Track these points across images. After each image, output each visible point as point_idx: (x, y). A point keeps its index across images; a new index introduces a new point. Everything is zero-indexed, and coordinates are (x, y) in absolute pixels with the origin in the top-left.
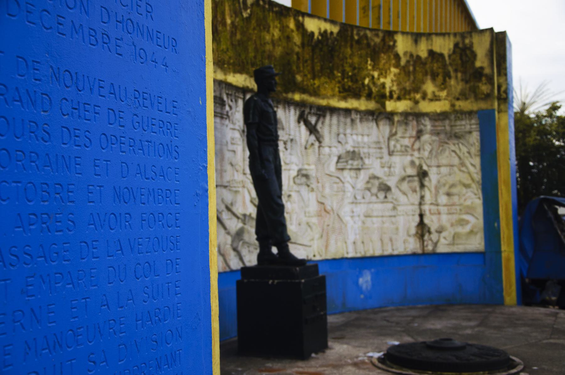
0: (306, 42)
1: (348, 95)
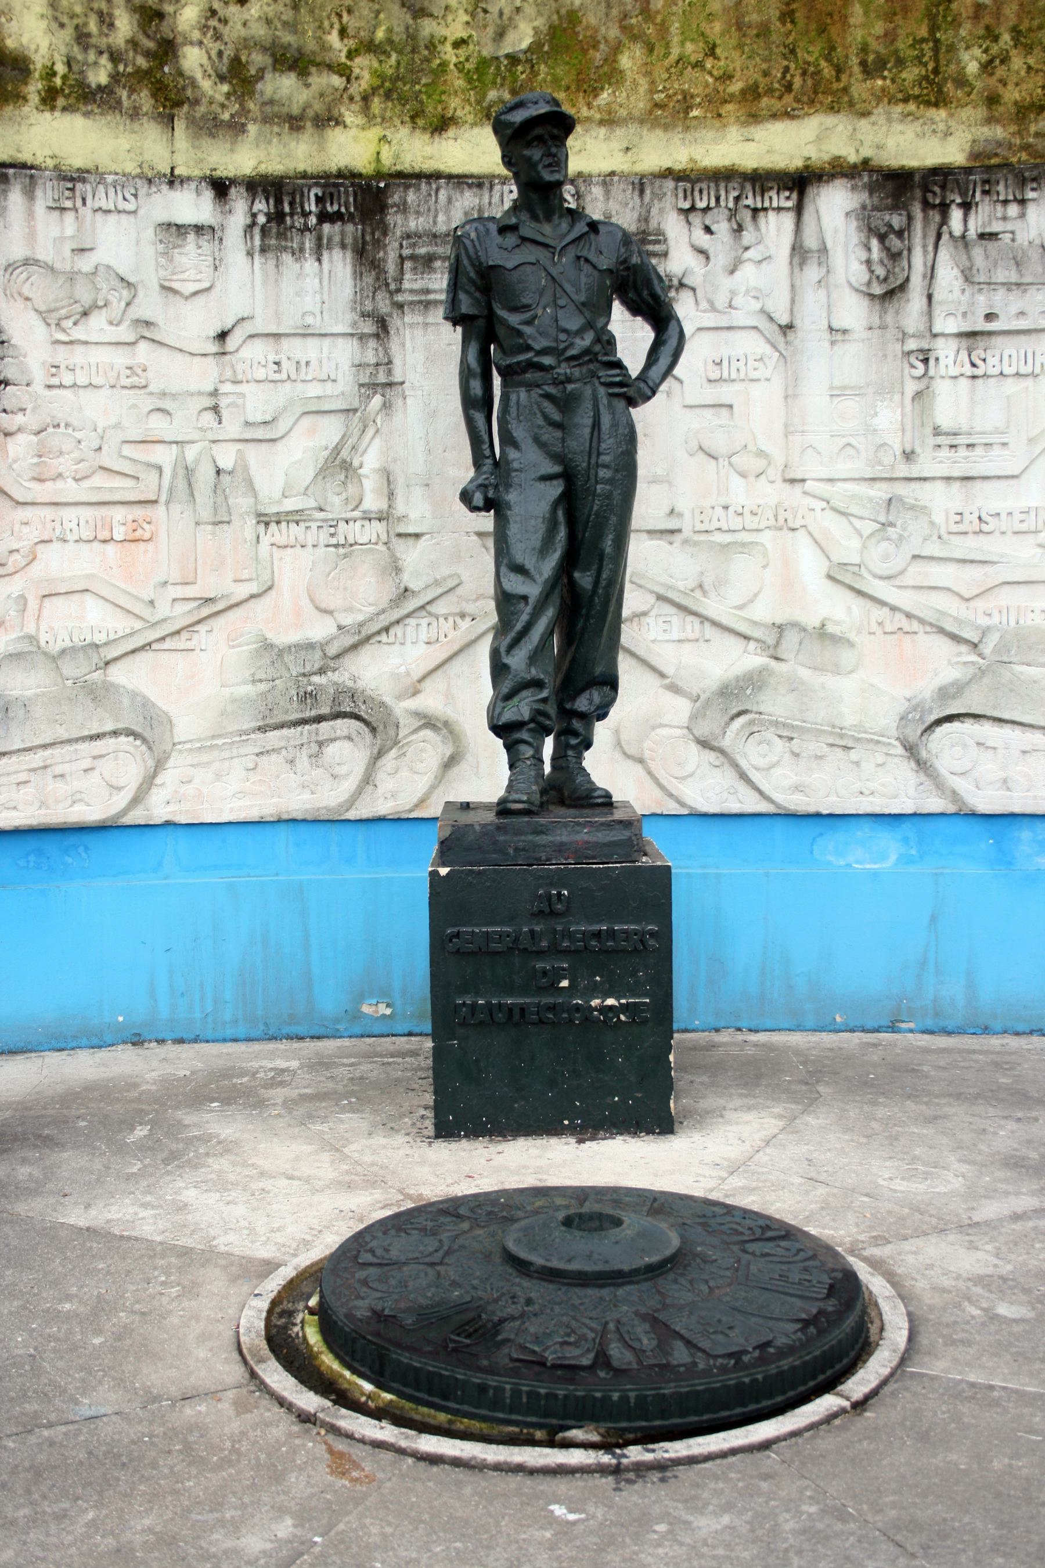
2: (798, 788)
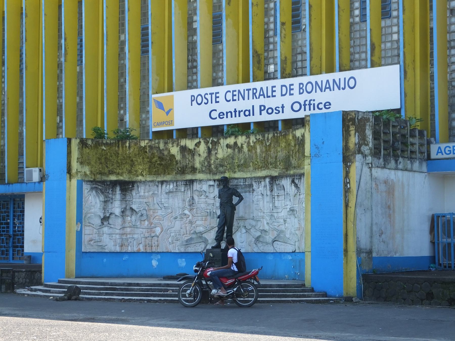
2: (263, 249)
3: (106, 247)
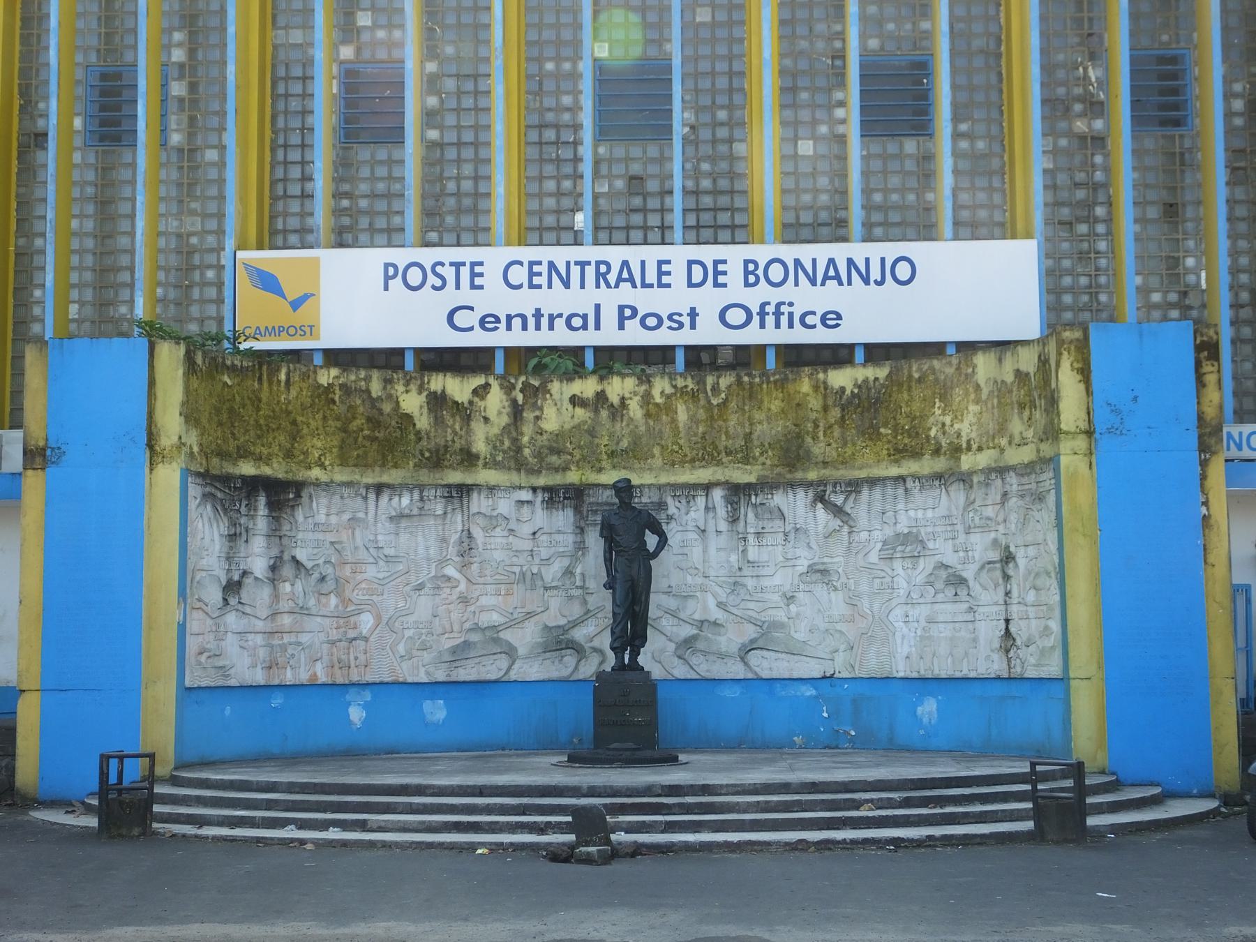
0: (830, 402)
1: (903, 457)
3: (232, 672)
